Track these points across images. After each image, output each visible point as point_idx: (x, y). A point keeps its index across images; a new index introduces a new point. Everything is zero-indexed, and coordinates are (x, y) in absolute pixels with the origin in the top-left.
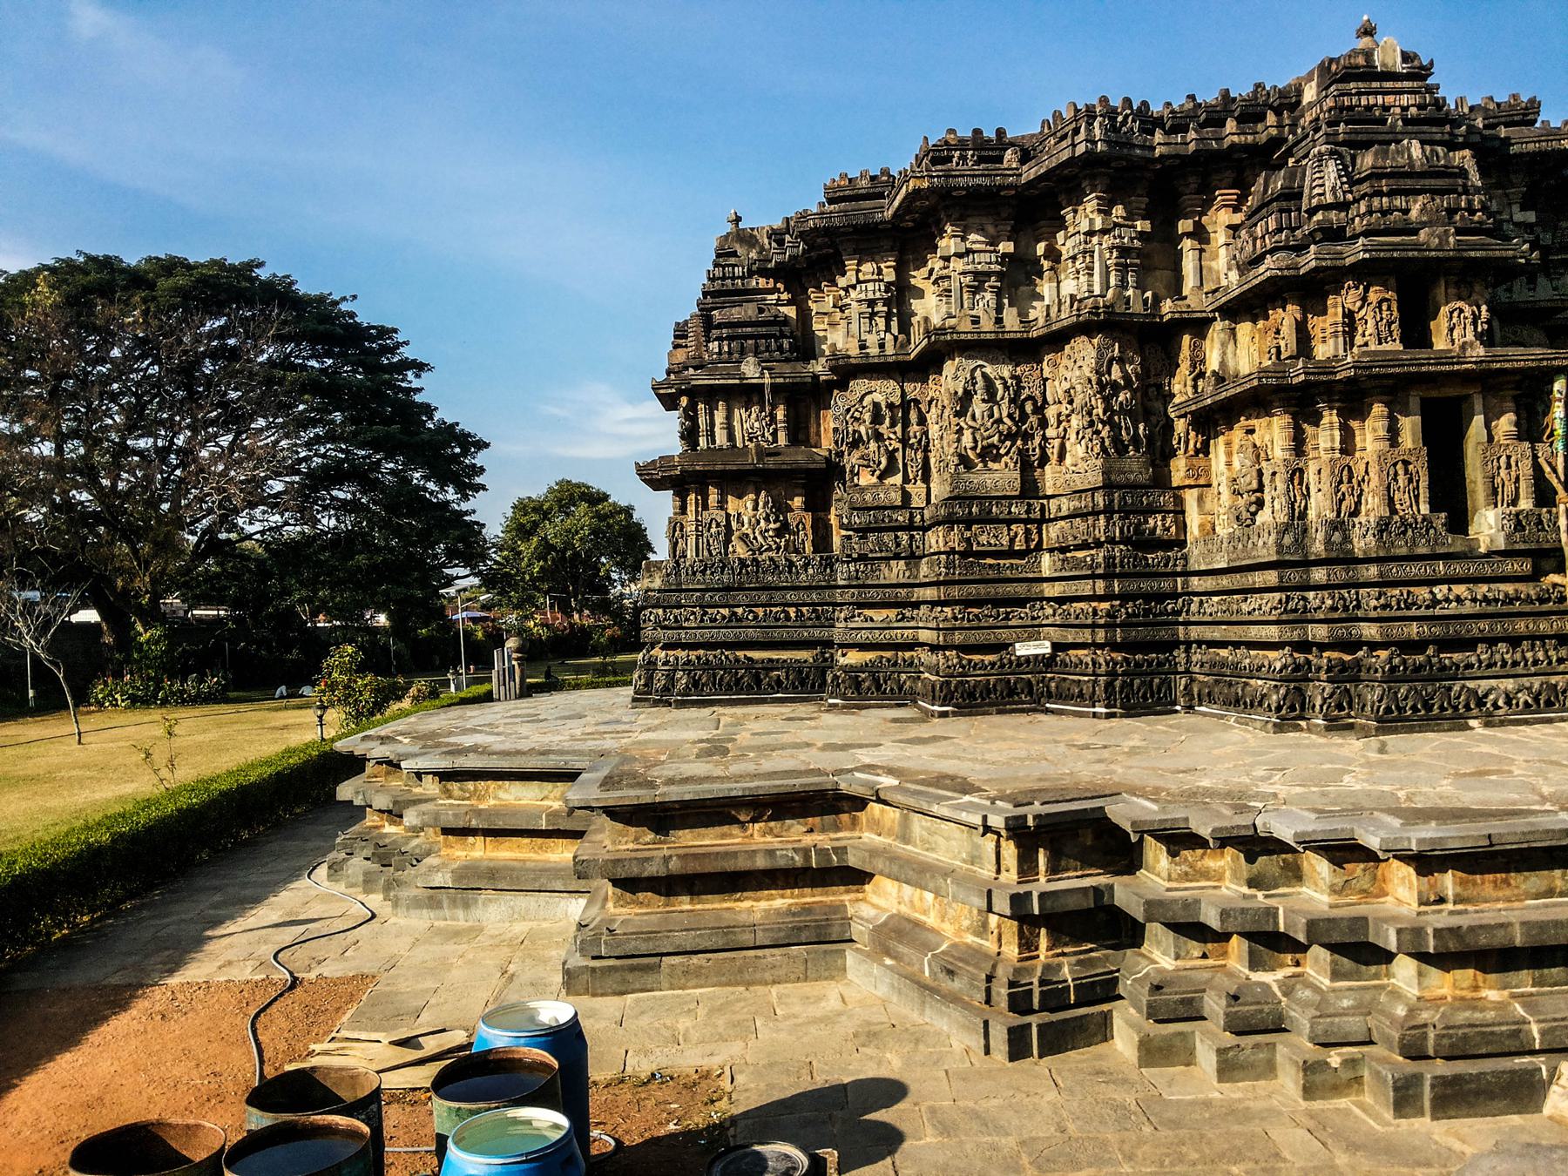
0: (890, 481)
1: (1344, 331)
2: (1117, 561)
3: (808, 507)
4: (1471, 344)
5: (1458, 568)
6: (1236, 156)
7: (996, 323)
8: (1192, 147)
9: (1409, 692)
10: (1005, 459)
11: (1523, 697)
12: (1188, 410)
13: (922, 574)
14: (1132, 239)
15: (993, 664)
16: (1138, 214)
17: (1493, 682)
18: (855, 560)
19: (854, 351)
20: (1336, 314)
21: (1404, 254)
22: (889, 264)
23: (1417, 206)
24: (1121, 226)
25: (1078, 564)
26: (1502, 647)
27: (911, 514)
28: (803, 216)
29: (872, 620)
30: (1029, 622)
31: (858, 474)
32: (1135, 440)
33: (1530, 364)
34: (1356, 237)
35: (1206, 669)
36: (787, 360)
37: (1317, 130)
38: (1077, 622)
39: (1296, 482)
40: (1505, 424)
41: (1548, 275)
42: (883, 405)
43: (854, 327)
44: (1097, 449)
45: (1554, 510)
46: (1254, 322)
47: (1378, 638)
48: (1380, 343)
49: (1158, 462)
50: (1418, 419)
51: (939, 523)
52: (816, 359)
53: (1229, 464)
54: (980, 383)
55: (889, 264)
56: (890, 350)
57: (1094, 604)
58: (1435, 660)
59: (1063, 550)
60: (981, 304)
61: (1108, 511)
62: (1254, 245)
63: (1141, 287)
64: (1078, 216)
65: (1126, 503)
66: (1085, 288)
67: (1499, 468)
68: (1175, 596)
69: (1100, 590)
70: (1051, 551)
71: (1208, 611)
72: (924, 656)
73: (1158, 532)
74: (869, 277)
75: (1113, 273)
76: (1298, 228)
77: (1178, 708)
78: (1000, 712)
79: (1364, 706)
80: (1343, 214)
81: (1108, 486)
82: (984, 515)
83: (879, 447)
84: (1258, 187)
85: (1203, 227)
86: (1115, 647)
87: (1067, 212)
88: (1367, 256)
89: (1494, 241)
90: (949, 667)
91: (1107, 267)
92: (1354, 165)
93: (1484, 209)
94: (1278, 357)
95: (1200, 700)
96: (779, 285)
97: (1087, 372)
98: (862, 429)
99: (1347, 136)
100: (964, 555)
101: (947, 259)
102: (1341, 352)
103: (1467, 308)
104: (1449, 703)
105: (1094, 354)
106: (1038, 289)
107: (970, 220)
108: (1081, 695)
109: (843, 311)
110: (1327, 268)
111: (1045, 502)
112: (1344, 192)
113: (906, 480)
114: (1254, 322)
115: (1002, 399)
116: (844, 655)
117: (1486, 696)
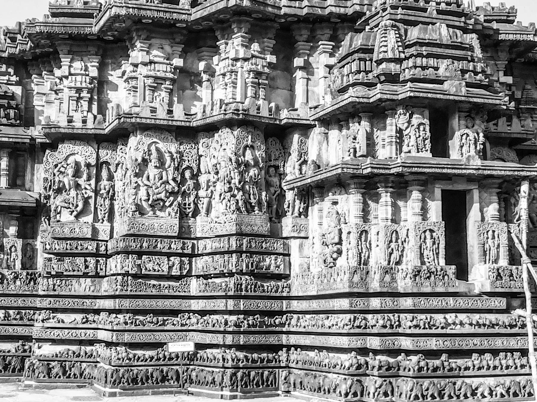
0: (83, 219)
1: (396, 142)
2: (243, 287)
3: (20, 235)
4: (473, 157)
5: (461, 303)
6: (333, 20)
7: (168, 113)
8: (305, 11)
9: (430, 385)
10: (169, 209)
11: (500, 390)
12: (295, 185)
13: (103, 289)
14: (263, 67)
15: (152, 358)
16: (268, 50)
17: (481, 380)
18: (53, 277)
19: (63, 123)
20: (392, 130)
21: (434, 96)
22: (93, 64)
23: (443, 66)
24: (257, 57)
25: (215, 287)
26: (488, 356)
27: (97, 244)
28: (32, 23)
29: (63, 322)
30: (179, 328)
31: (60, 213)
32: (260, 203)
33: (508, 173)
34: (406, 81)
35: (300, 365)
36: (12, 125)
37: (384, 10)
38: (213, 329)
39: (363, 239)
40: (492, 210)
41: (519, 117)
42: (83, 164)
43: (65, 106)
44: (233, 207)
45: (520, 267)
46: (340, 130)
47: (411, 348)
48: (418, 152)
49: (273, 219)
50: (440, 203)
51: (118, 253)
52: (33, 126)
53: (320, 224)
54: (154, 154)
55: (93, 64)
56: (90, 124)
57: (226, 317)
58: (446, 364)
59: (206, 277)
60: (158, 99)
61: (239, 252)
62: (342, 80)
63: (267, 99)
64: (228, 47)
65: (251, 247)
66: (230, 96)
67: (488, 238)
68: (281, 313)
69: (230, 308)
70: (198, 277)
71: (303, 325)
72: (100, 349)
73: (272, 268)
74: (78, 72)
75: (250, 88)
76: (371, 71)
77: (279, 392)
78: (154, 394)
79: (401, 394)
80: (398, 66)
81: (240, 234)
82: (151, 249)
83: (77, 194)
84: (346, 42)
85: (310, 64)
86: (240, 348)
87: (221, 43)
88: (412, 94)
89: (488, 93)
90: (119, 359)
91: (246, 83)
92: (406, 36)
93: (483, 72)
94: (355, 156)
95: (295, 387)
96: (10, 70)
97: (229, 153)
98: (66, 181)
99: (402, 17)
100: (135, 276)
101: (136, 65)
102: (394, 156)
103: (472, 135)
104: (455, 393)
105: (234, 141)
106: (198, 93)
107: (153, 41)
108: (214, 382)
109: (57, 94)
110: (388, 100)
111: (195, 242)
112: (399, 52)
113: (96, 219)
114: (340, 130)
115: (169, 167)
116: (39, 348)
117: (477, 389)
